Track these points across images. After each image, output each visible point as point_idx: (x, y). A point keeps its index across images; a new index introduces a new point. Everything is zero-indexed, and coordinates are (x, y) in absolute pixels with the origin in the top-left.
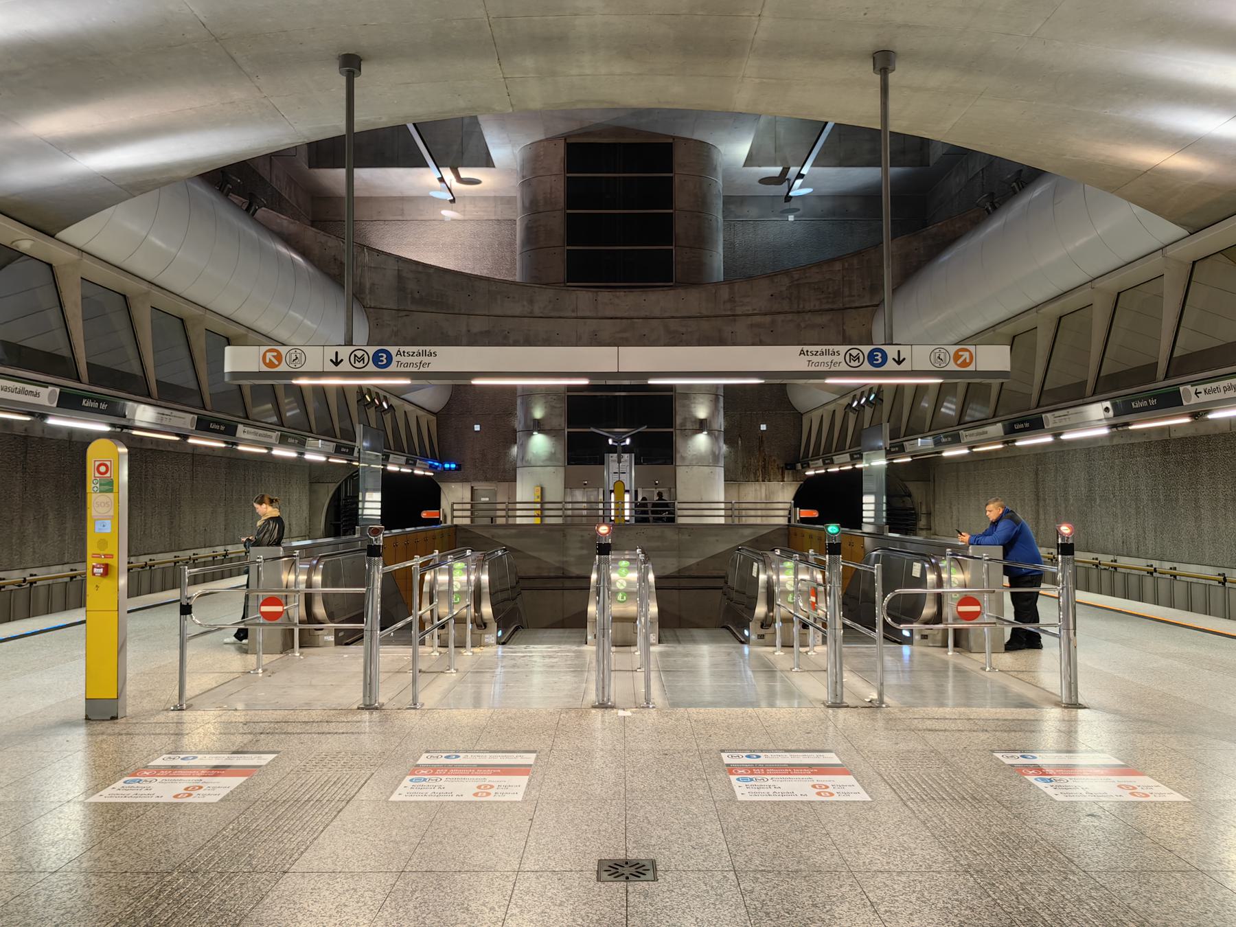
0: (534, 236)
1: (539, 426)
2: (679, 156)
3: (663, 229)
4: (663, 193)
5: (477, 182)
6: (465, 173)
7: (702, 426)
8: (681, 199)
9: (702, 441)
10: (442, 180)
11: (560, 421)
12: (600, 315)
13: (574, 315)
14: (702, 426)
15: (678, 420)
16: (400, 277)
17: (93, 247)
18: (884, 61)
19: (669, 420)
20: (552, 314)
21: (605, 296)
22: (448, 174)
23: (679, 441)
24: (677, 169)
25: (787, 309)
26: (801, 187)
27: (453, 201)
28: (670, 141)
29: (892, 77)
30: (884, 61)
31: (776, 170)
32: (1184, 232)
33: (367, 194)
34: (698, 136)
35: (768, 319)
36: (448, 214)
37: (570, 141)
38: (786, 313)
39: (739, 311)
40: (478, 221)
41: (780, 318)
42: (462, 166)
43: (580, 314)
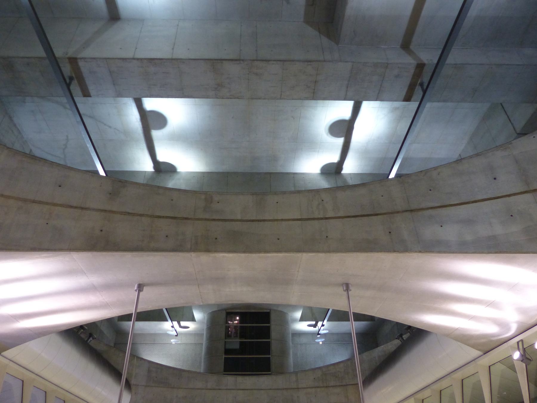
0: (211, 352)
2: (273, 317)
3: (266, 348)
4: (266, 332)
5: (188, 327)
6: (183, 323)
8: (274, 334)
10: (173, 327)
16: (149, 371)
17: (18, 359)
18: (347, 287)
21: (240, 379)
22: (175, 323)
24: (272, 323)
26: (323, 330)
27: (177, 336)
28: (268, 311)
29: (350, 292)
30: (347, 287)
31: (314, 323)
32: (476, 353)
33: (139, 332)
34: (281, 310)
35: (314, 390)
36: (173, 341)
37: (228, 311)
38: (321, 387)
39: (300, 386)
40: (186, 344)
41: (319, 390)
43: (228, 388)
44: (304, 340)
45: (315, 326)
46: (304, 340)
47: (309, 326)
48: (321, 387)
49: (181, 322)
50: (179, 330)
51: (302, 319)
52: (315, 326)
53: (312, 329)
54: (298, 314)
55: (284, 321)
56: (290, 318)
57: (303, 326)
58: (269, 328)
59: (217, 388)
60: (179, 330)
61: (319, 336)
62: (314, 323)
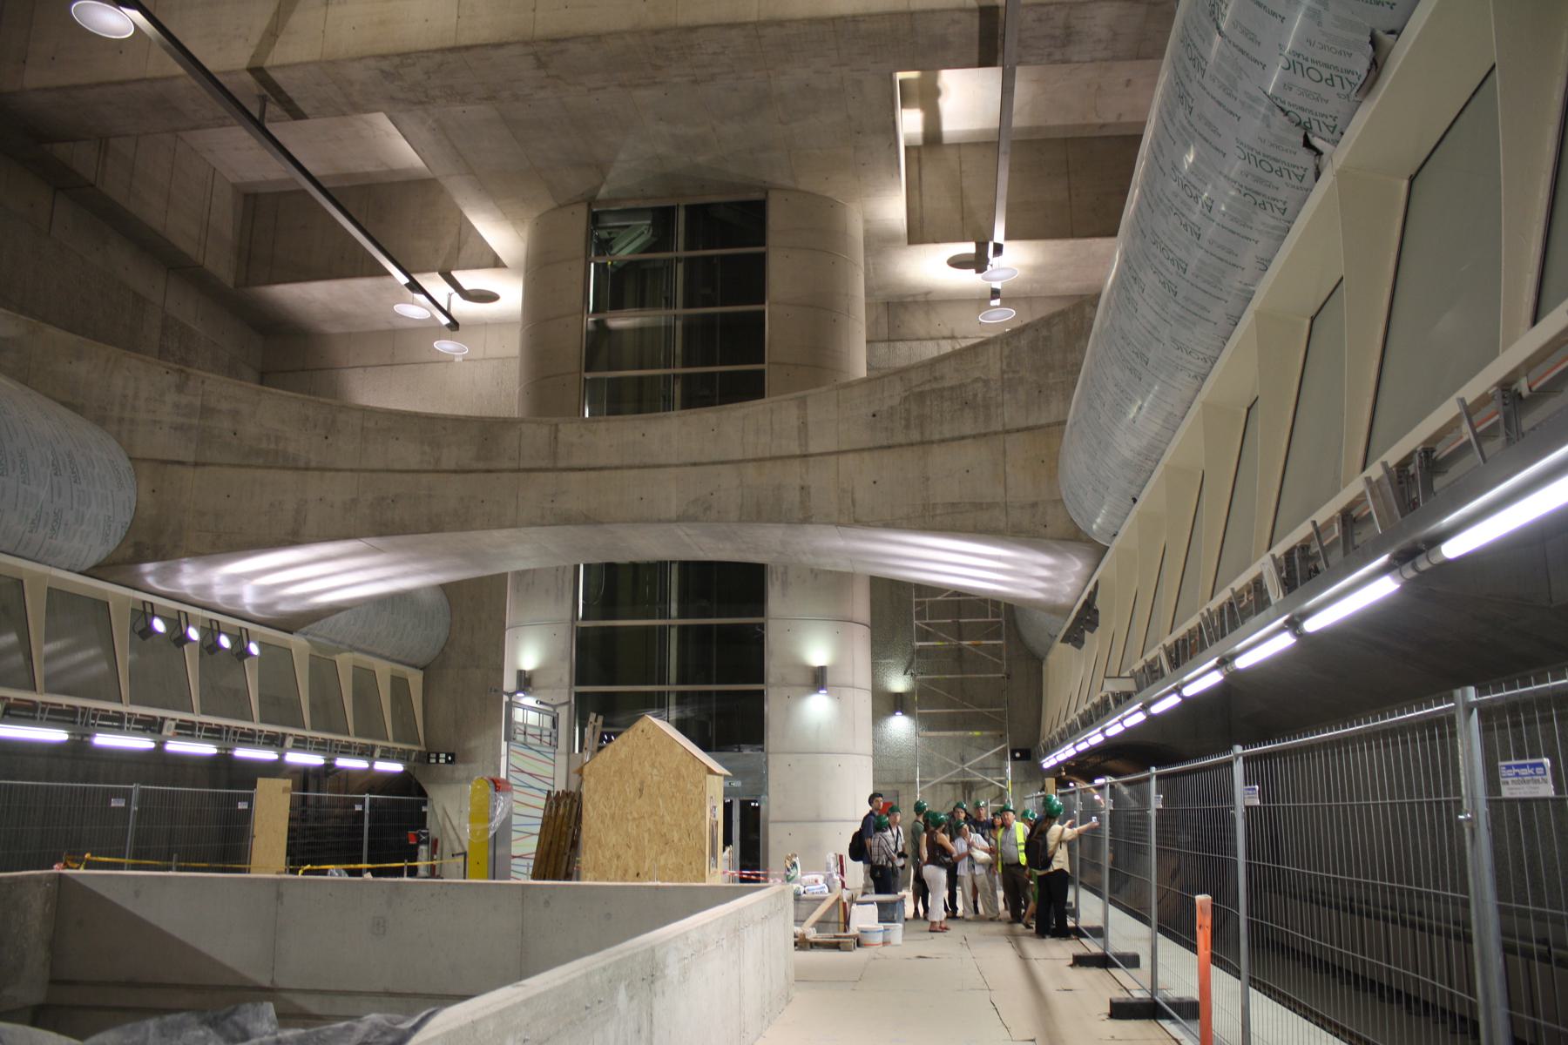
1: (526, 682)
2: (777, 217)
6: (470, 279)
7: (818, 679)
9: (817, 708)
10: (415, 287)
11: (565, 672)
12: (562, 464)
13: (514, 465)
14: (818, 679)
15: (773, 667)
19: (756, 672)
20: (476, 465)
23: (772, 708)
25: (900, 438)
28: (756, 196)
31: (969, 248)
34: (805, 183)
36: (445, 346)
42: (458, 269)
43: (524, 464)
44: (946, 321)
45: (978, 263)
46: (946, 321)
47: (957, 263)
48: (901, 446)
49: (454, 273)
50: (461, 307)
51: (919, 233)
52: (978, 263)
53: (968, 279)
54: (893, 208)
55: (824, 231)
56: (857, 230)
57: (930, 267)
58: (760, 261)
59: (481, 465)
60: (461, 307)
61: (997, 302)
62: (969, 248)
